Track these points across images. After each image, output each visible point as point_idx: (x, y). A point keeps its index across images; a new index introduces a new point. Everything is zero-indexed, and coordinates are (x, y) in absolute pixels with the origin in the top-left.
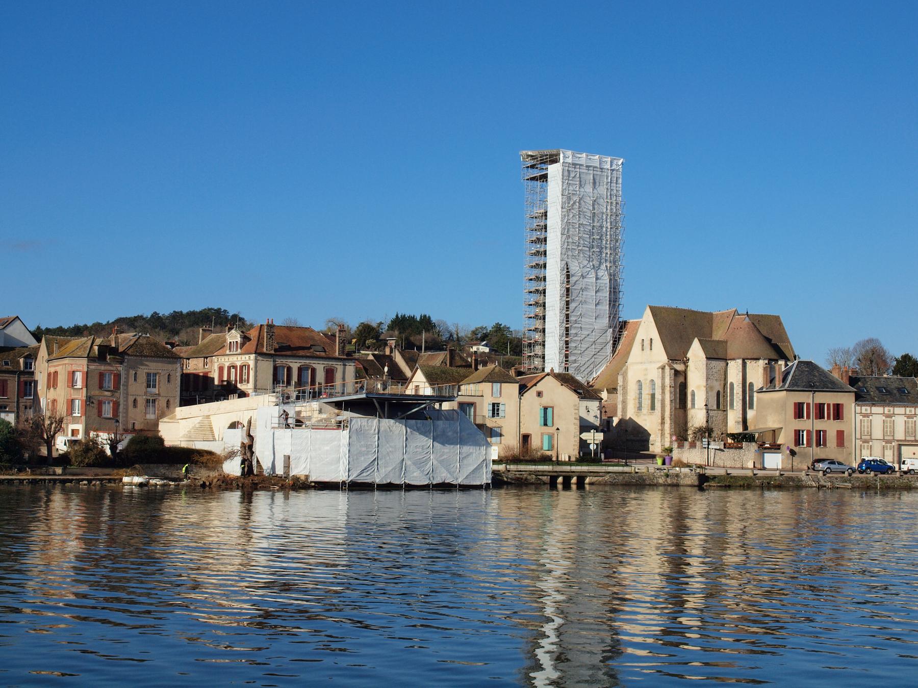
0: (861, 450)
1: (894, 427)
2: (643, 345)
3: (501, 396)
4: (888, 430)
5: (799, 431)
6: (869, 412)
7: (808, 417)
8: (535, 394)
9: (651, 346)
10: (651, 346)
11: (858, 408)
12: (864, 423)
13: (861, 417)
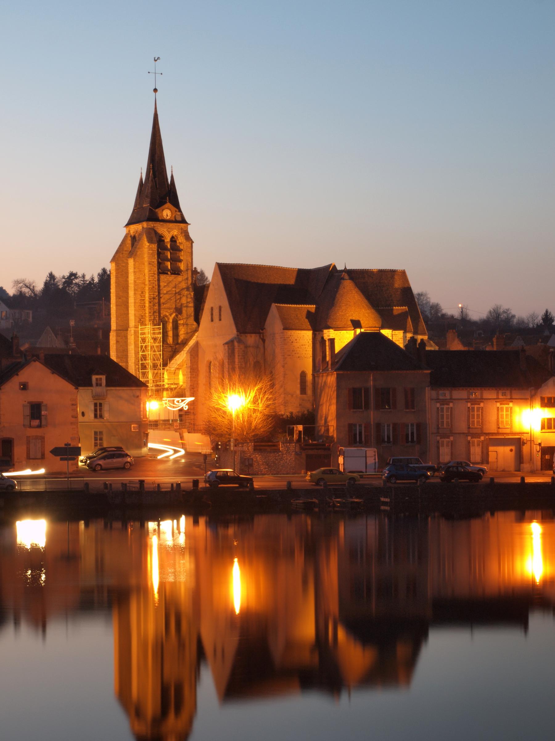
0: (438, 448)
1: (482, 415)
2: (212, 314)
4: (476, 420)
5: (355, 425)
6: (448, 397)
7: (367, 407)
9: (220, 315)
10: (220, 315)
11: (434, 393)
12: (442, 411)
13: (438, 405)
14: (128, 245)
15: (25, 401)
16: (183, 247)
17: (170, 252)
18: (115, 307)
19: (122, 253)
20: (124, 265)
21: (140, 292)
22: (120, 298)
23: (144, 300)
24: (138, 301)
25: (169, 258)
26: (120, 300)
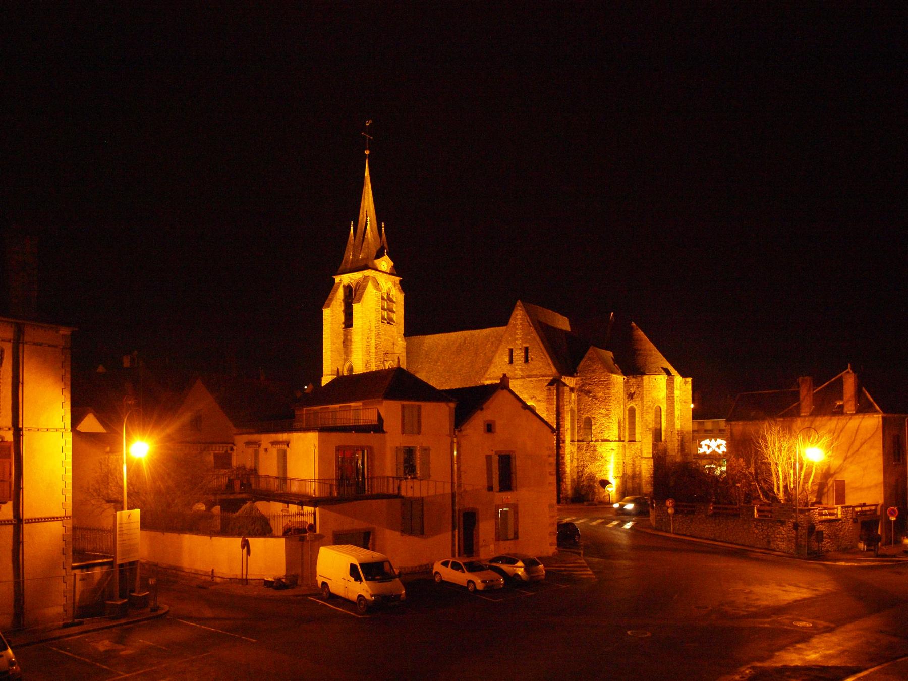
3: (419, 433)
8: (481, 428)
14: (340, 294)
15: (492, 451)
16: (396, 299)
17: (387, 302)
18: (329, 353)
19: (336, 301)
20: (337, 312)
21: (366, 338)
22: (334, 344)
23: (369, 345)
24: (364, 346)
25: (386, 308)
26: (335, 346)
